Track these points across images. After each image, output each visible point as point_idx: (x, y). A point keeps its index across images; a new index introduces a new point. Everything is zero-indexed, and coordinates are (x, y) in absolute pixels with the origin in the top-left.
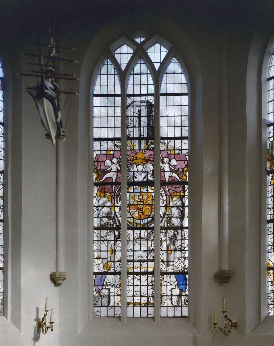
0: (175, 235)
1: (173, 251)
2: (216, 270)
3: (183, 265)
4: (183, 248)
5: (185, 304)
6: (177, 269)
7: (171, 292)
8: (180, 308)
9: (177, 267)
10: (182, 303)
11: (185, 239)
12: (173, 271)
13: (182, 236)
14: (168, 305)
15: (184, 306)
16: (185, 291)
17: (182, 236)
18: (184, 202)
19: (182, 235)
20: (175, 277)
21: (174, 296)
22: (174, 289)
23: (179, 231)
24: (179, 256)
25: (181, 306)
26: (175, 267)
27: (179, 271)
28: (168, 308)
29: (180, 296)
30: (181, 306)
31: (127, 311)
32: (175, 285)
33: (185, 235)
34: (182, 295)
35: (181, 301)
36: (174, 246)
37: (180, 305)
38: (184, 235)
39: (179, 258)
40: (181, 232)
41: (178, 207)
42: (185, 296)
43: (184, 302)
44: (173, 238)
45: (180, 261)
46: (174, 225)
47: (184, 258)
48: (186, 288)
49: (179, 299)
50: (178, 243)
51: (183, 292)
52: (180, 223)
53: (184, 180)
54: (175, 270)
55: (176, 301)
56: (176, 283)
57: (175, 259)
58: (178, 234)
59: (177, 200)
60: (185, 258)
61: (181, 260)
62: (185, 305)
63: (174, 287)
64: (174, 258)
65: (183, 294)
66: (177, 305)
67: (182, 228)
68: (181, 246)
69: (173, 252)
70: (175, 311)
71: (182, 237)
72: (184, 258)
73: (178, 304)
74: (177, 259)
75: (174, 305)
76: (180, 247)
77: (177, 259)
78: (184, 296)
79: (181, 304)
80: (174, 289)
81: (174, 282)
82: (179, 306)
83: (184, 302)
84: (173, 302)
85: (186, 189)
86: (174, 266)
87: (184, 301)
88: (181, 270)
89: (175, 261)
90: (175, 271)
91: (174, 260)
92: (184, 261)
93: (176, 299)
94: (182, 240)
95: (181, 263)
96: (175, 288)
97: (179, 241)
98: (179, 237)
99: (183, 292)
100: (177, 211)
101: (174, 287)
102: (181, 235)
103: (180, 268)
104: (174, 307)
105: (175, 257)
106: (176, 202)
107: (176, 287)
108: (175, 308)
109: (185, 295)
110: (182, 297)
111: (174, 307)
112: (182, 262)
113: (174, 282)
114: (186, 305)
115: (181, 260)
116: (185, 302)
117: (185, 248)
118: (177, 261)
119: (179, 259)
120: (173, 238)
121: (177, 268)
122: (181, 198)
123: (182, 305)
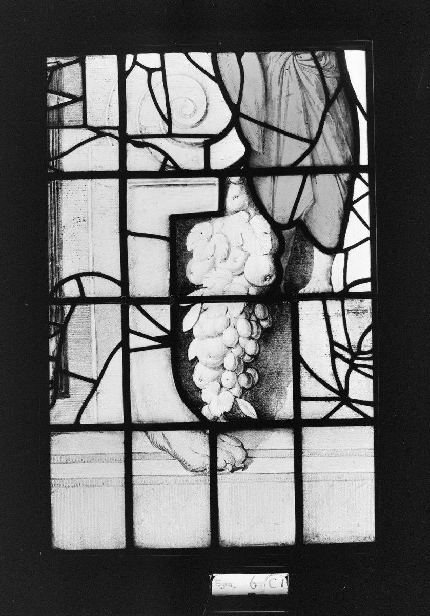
5: (342, 396)
8: (283, 440)
10: (309, 387)
14: (140, 413)
15: (326, 421)
20: (218, 78)
25: (297, 425)
28: (140, 441)
30: (297, 425)
32: (223, 176)
34: (309, 289)
35: (298, 361)
37: (283, 408)
42: (334, 306)
49: (266, 337)
55: (230, 362)
62: (346, 412)
66: (248, 410)
73: (251, 393)
78: (323, 297)
79: (298, 398)
81: (210, 140)
82: (265, 422)
83: (326, 373)
84: (201, 376)
87: (334, 355)
93: (229, 337)
96: (222, 212)
107: (236, 193)
108: (228, 448)
110: (309, 311)
113: (210, 140)
114: (349, 402)
116: (343, 368)
123: (310, 410)
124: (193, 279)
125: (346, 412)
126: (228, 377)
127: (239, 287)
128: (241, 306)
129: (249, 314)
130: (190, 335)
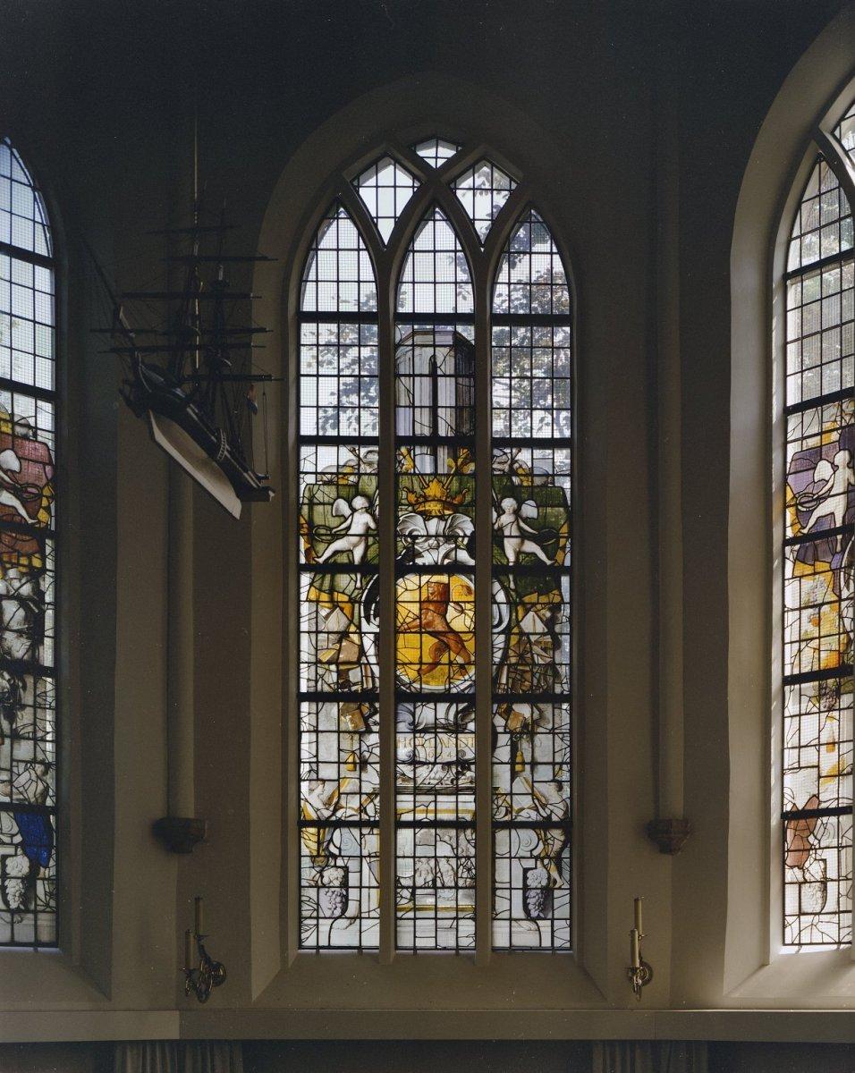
0: (14, 688)
1: (7, 737)
2: (158, 811)
3: (41, 787)
4: (40, 734)
5: (47, 905)
6: (21, 797)
7: (525, 878)
8: (31, 916)
9: (21, 789)
10: (39, 902)
11: (48, 706)
12: (7, 800)
13: (38, 696)
14: (514, 916)
15: (44, 911)
16: (46, 867)
17: (38, 696)
18: (42, 588)
19: (38, 693)
20: (15, 819)
21: (13, 878)
22: (532, 869)
23: (30, 680)
24: (28, 756)
25: (35, 912)
26: (14, 790)
27: (29, 802)
28: (514, 923)
29: (29, 881)
30: (35, 912)
31: (492, 933)
32: (16, 846)
33: (48, 694)
34: (40, 876)
35: (36, 896)
36: (11, 724)
38: (45, 692)
39: (27, 762)
40: (35, 684)
41: (22, 601)
42: (46, 882)
43: (42, 897)
44: (8, 699)
45: (32, 772)
46: (9, 653)
47: (42, 762)
48: (50, 856)
50: (25, 717)
51: (42, 869)
52: (30, 653)
53: (42, 525)
54: (14, 797)
55: (17, 894)
56: (18, 839)
57: (14, 764)
58: (24, 688)
59: (20, 580)
60: (47, 766)
61: (34, 769)
62: (48, 909)
63: (10, 850)
64: (12, 760)
65: (41, 875)
66: (22, 907)
67: (39, 671)
68: (34, 724)
69: (7, 741)
70: (16, 926)
71: (39, 700)
72: (42, 762)
74: (22, 766)
75: (14, 905)
76: (30, 729)
77: (22, 766)
78: (43, 879)
79: (36, 905)
80: (532, 869)
81: (12, 836)
84: (10, 898)
85: (48, 549)
86: (12, 786)
87: (46, 895)
88: (33, 800)
89: (15, 770)
90: (14, 802)
91: (12, 766)
92: (45, 773)
93: (17, 888)
94: (35, 706)
95: (34, 777)
96: (536, 868)
97: (28, 708)
98: (28, 698)
99: (42, 869)
100: (21, 613)
101: (10, 850)
102: (35, 693)
103: (31, 794)
104: (13, 912)
105: (15, 758)
106: (16, 584)
108: (17, 918)
109: (48, 879)
110: (39, 884)
111: (13, 912)
112: (38, 777)
113: (12, 836)
114: (50, 907)
115: (34, 769)
116: (48, 898)
117: (48, 733)
118: (21, 770)
119: (29, 765)
120: (8, 699)
121: (21, 793)
122: (34, 575)
123: (39, 908)
124: (8, 872)
125: (48, 909)
126: (17, 898)
127: (20, 875)
128: (20, 881)
129: (22, 882)
130: (6, 887)
